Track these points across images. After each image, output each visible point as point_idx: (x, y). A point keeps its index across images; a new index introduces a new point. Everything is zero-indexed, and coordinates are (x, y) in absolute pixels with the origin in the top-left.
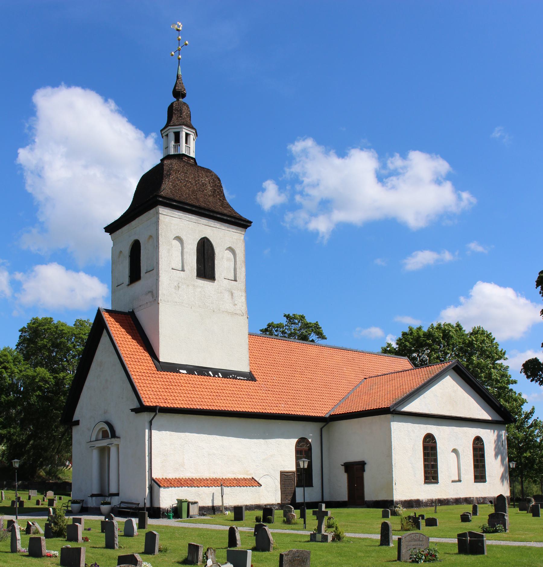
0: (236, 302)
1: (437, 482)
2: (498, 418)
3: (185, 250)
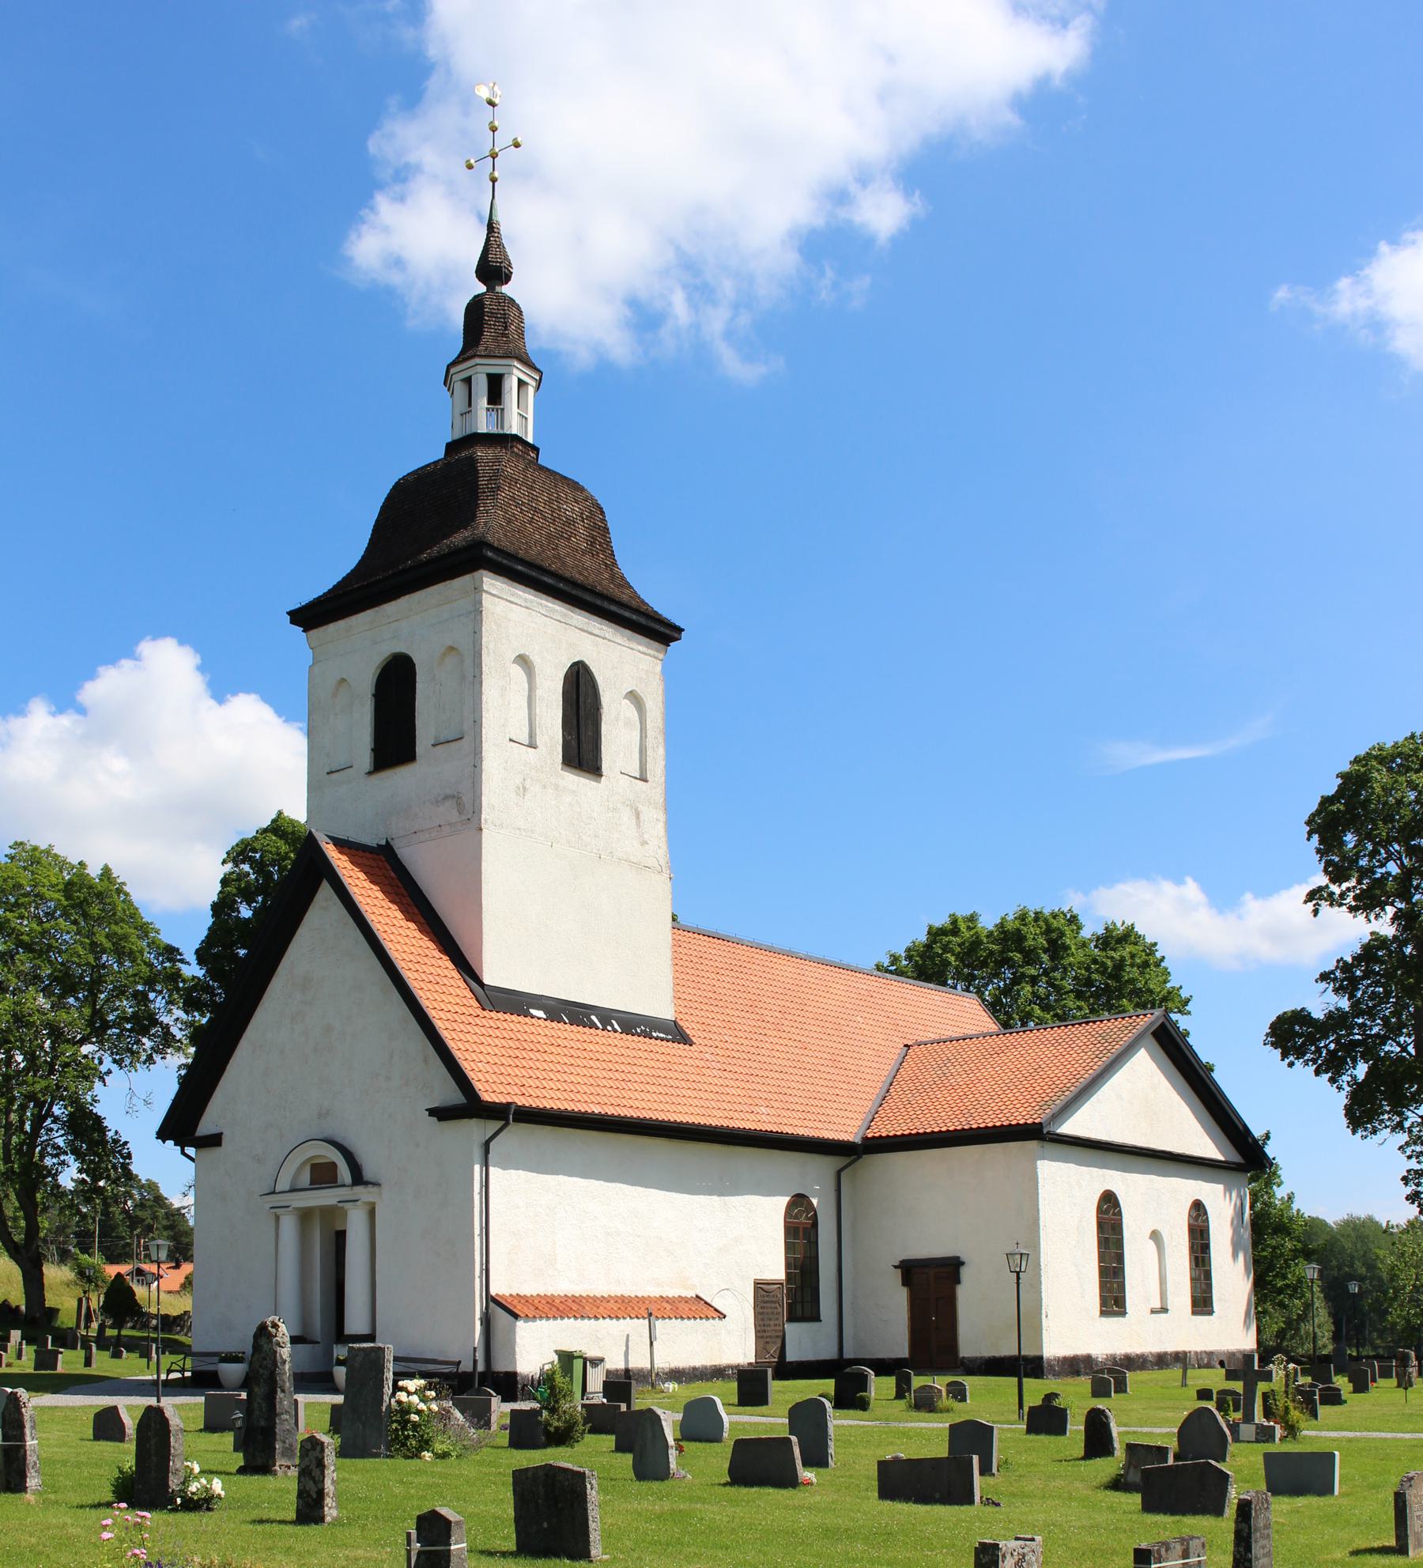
0: (646, 836)
1: (1123, 1313)
2: (1236, 1158)
3: (539, 692)
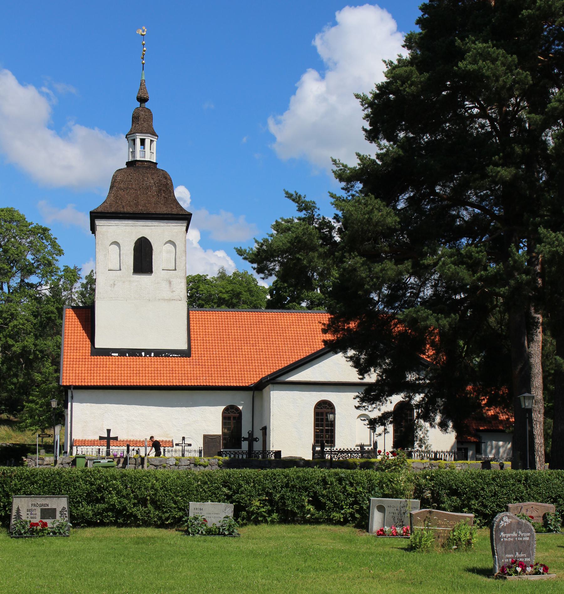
0: (174, 289)
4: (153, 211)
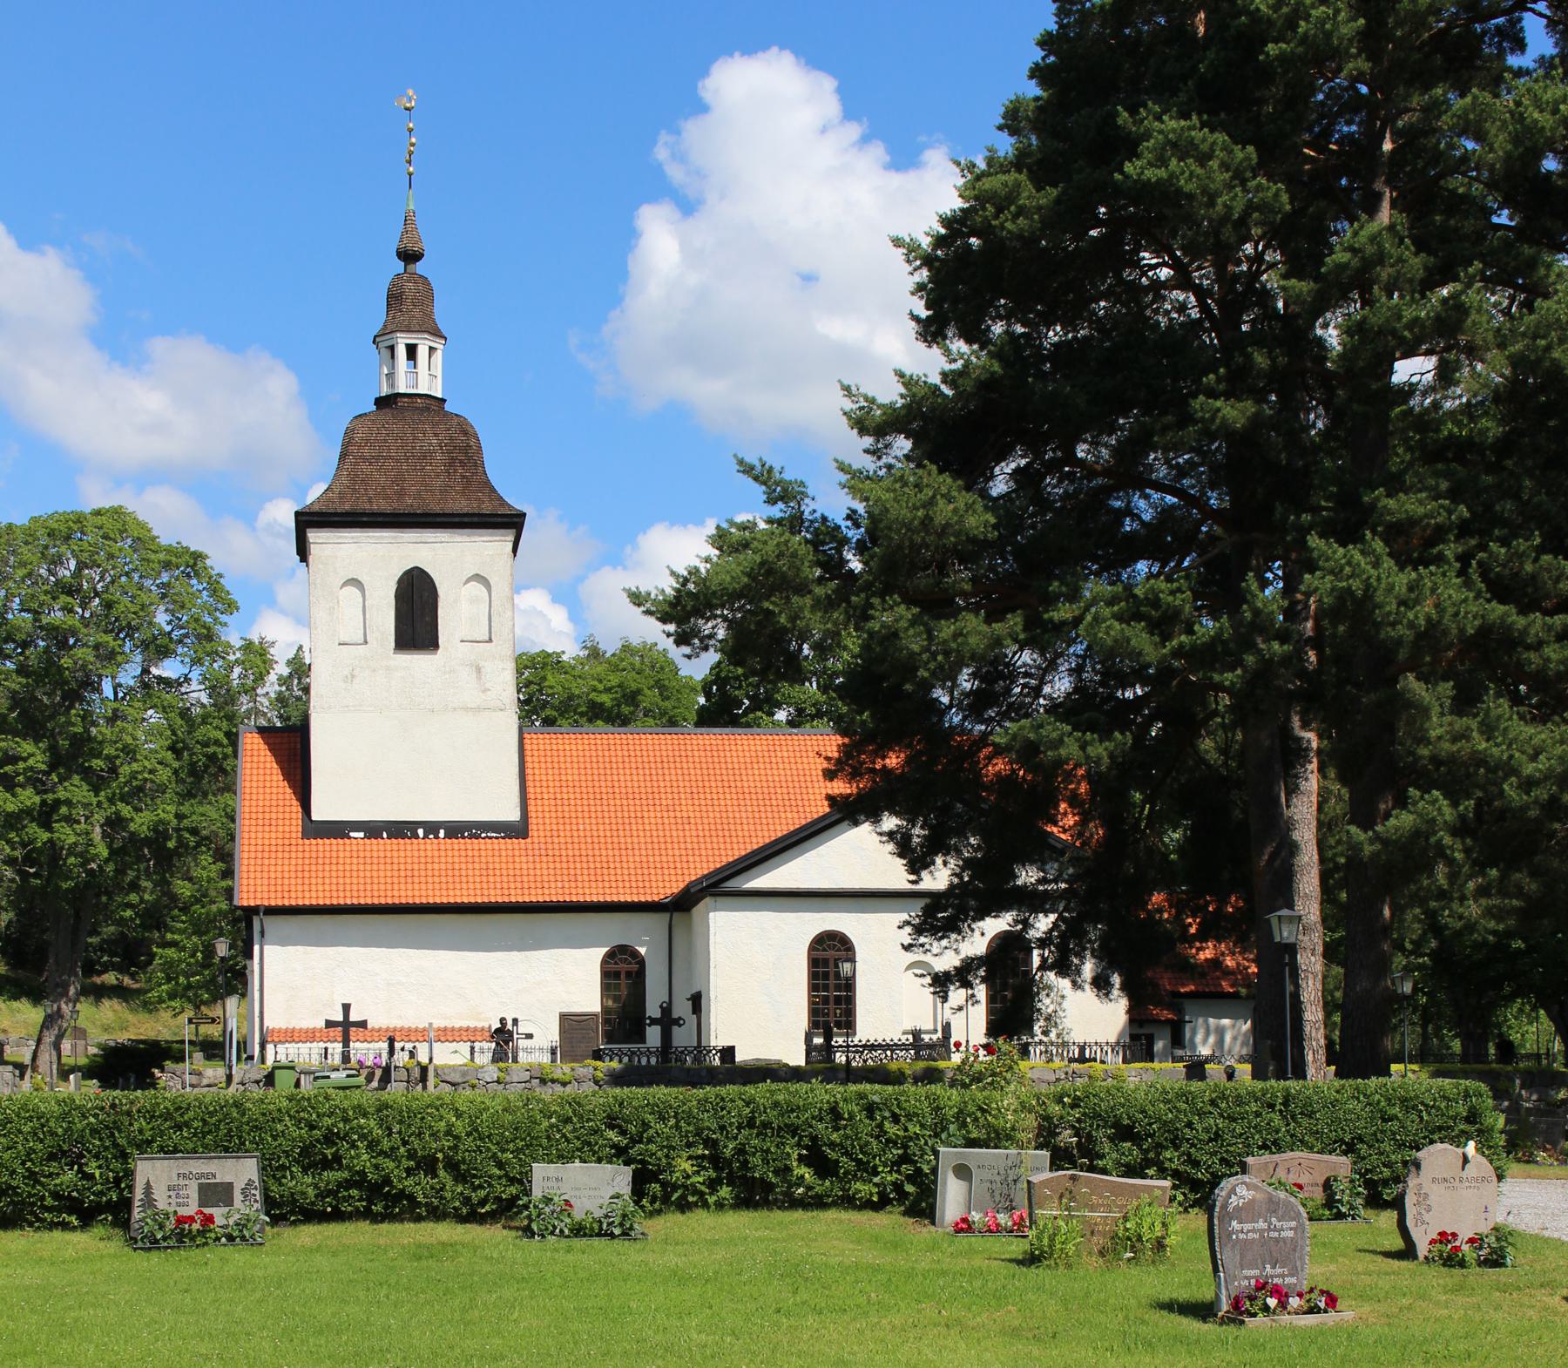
0: (488, 685)
4: (437, 509)
